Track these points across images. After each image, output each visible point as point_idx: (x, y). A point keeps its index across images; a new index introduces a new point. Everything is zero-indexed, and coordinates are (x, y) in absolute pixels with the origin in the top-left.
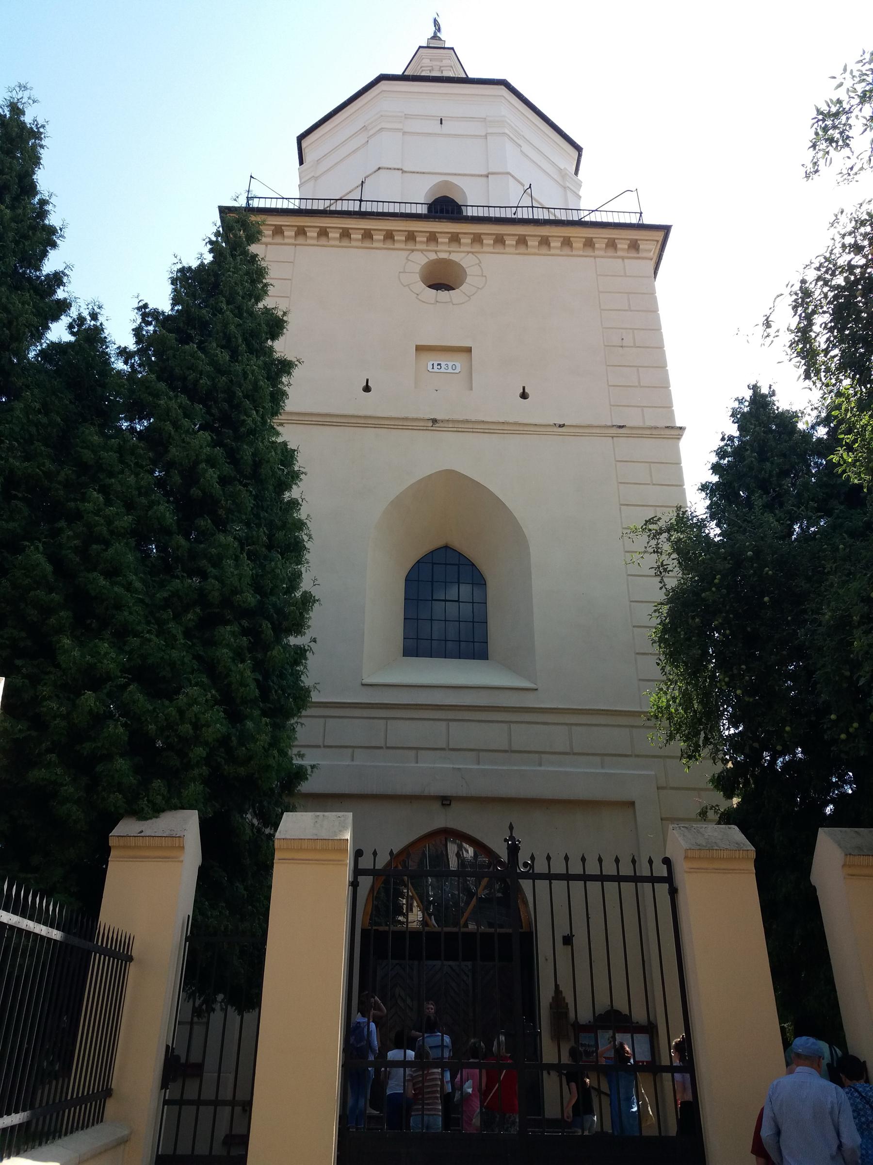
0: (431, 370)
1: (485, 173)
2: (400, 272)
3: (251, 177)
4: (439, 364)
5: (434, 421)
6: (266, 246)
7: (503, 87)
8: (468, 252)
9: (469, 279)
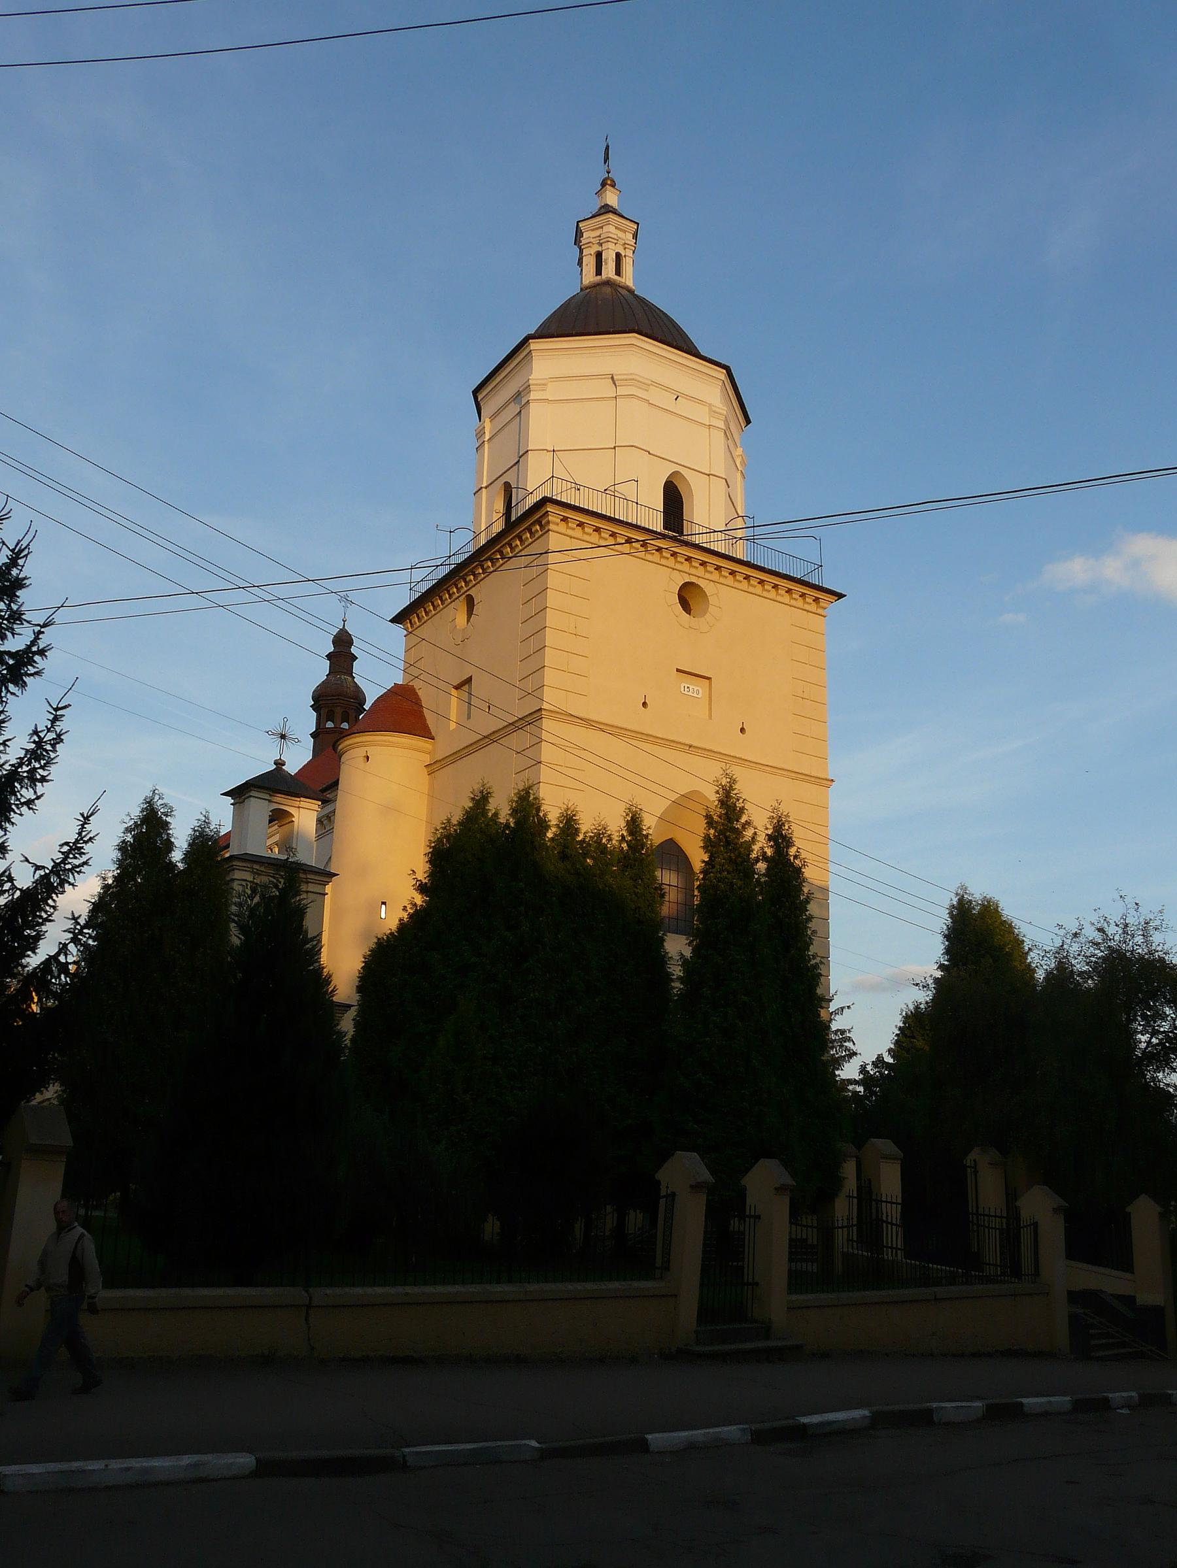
0: (683, 692)
1: (708, 473)
4: (688, 687)
5: (691, 746)
7: (725, 371)
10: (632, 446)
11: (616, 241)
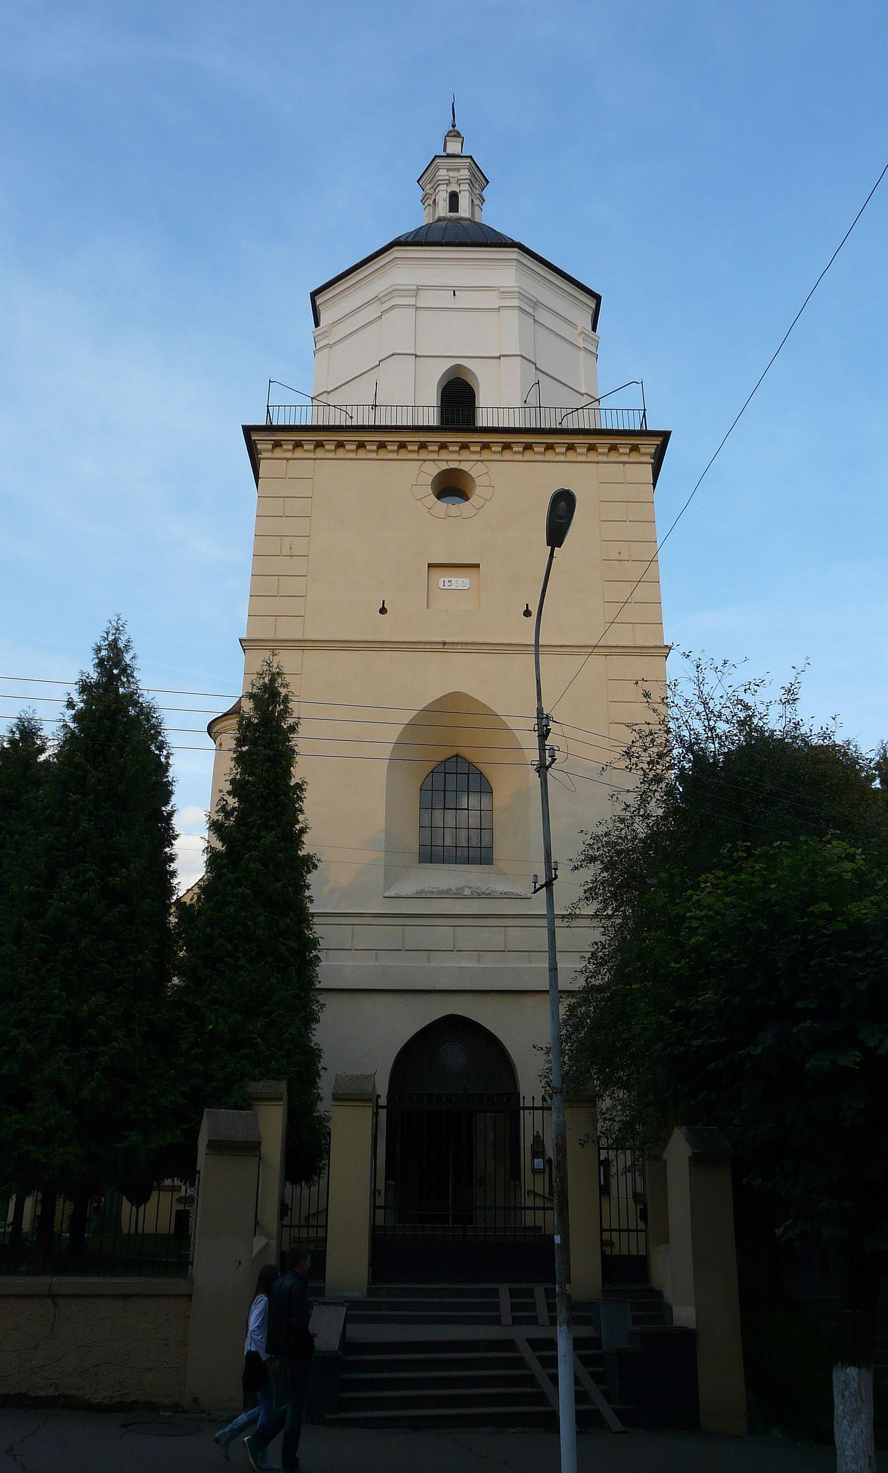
1: (498, 355)
2: (412, 485)
3: (270, 381)
4: (450, 581)
5: (444, 643)
6: (287, 460)
7: (516, 249)
8: (477, 461)
9: (478, 491)
10: (393, 355)
11: (447, 182)
